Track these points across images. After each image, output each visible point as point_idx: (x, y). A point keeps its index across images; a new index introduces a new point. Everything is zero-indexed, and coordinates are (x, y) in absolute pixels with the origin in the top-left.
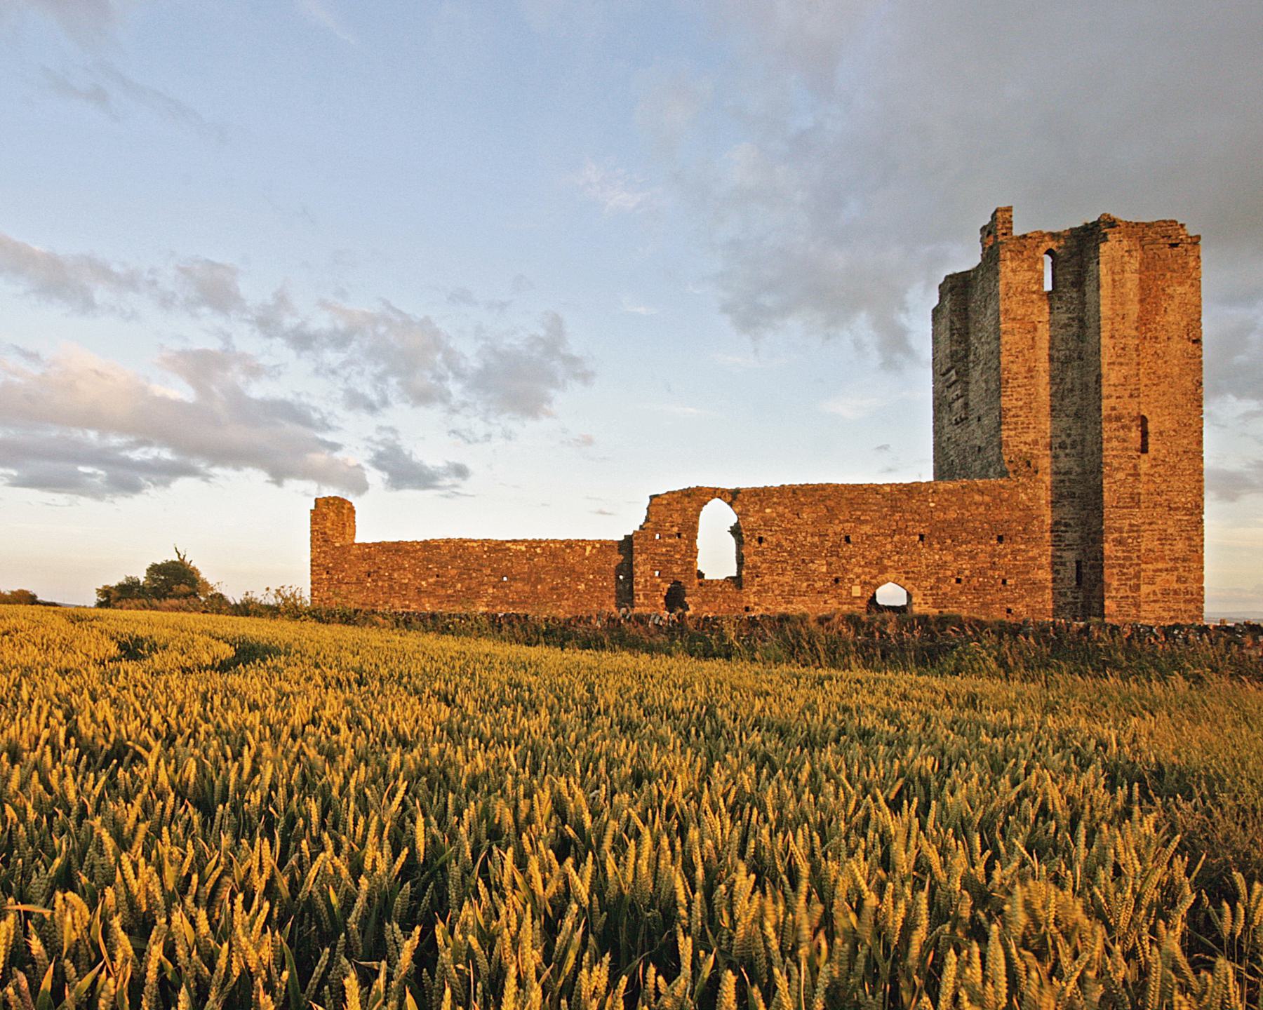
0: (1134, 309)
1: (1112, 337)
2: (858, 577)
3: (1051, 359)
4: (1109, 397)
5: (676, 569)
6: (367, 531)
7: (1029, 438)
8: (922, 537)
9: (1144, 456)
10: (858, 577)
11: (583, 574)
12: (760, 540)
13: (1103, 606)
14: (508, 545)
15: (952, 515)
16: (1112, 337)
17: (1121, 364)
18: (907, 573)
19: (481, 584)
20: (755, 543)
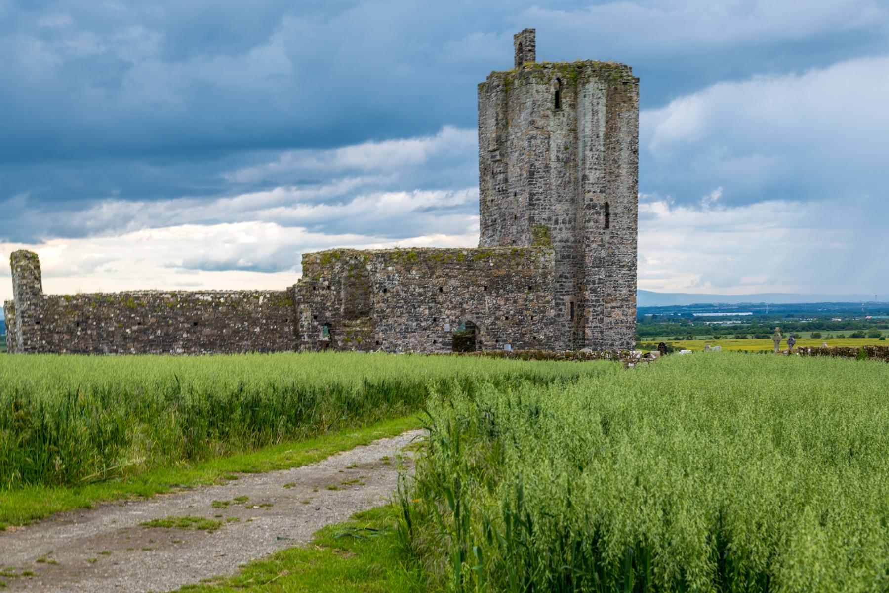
0: (602, 130)
1: (591, 150)
2: (448, 317)
3: (558, 160)
4: (589, 191)
5: (328, 314)
6: (50, 287)
7: (545, 216)
8: (486, 288)
9: (606, 231)
10: (448, 317)
11: (258, 319)
12: (385, 291)
13: (584, 332)
14: (197, 296)
15: (503, 272)
16: (591, 150)
17: (596, 169)
18: (477, 313)
19: (177, 329)
20: (381, 293)
